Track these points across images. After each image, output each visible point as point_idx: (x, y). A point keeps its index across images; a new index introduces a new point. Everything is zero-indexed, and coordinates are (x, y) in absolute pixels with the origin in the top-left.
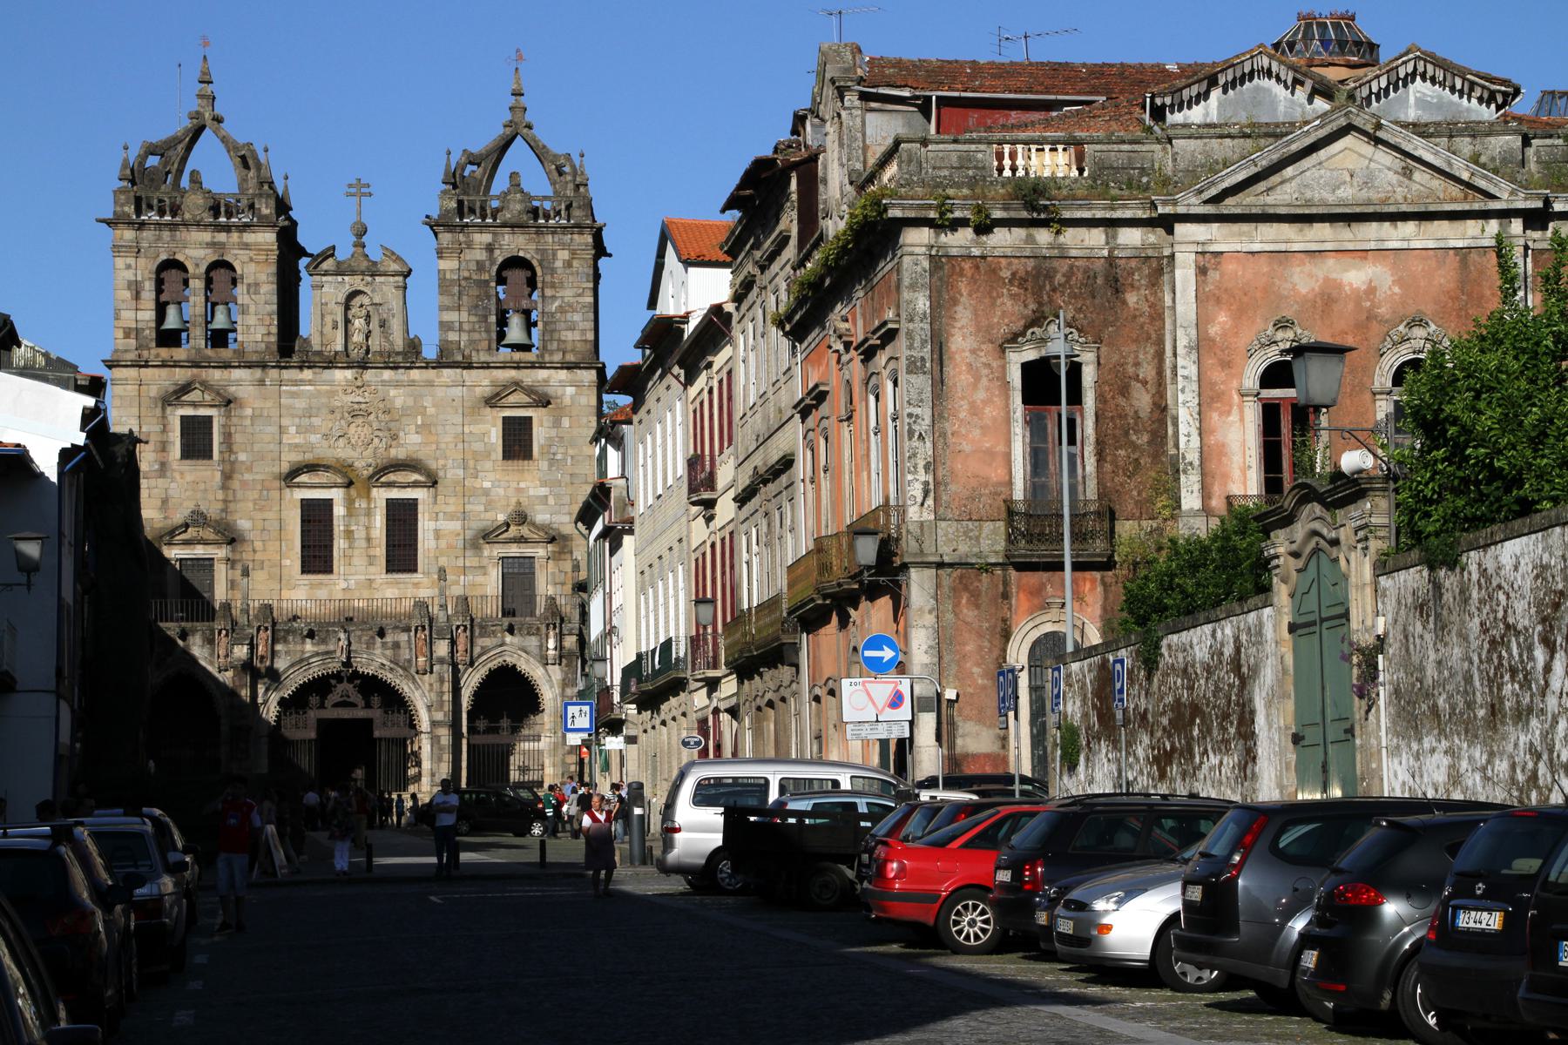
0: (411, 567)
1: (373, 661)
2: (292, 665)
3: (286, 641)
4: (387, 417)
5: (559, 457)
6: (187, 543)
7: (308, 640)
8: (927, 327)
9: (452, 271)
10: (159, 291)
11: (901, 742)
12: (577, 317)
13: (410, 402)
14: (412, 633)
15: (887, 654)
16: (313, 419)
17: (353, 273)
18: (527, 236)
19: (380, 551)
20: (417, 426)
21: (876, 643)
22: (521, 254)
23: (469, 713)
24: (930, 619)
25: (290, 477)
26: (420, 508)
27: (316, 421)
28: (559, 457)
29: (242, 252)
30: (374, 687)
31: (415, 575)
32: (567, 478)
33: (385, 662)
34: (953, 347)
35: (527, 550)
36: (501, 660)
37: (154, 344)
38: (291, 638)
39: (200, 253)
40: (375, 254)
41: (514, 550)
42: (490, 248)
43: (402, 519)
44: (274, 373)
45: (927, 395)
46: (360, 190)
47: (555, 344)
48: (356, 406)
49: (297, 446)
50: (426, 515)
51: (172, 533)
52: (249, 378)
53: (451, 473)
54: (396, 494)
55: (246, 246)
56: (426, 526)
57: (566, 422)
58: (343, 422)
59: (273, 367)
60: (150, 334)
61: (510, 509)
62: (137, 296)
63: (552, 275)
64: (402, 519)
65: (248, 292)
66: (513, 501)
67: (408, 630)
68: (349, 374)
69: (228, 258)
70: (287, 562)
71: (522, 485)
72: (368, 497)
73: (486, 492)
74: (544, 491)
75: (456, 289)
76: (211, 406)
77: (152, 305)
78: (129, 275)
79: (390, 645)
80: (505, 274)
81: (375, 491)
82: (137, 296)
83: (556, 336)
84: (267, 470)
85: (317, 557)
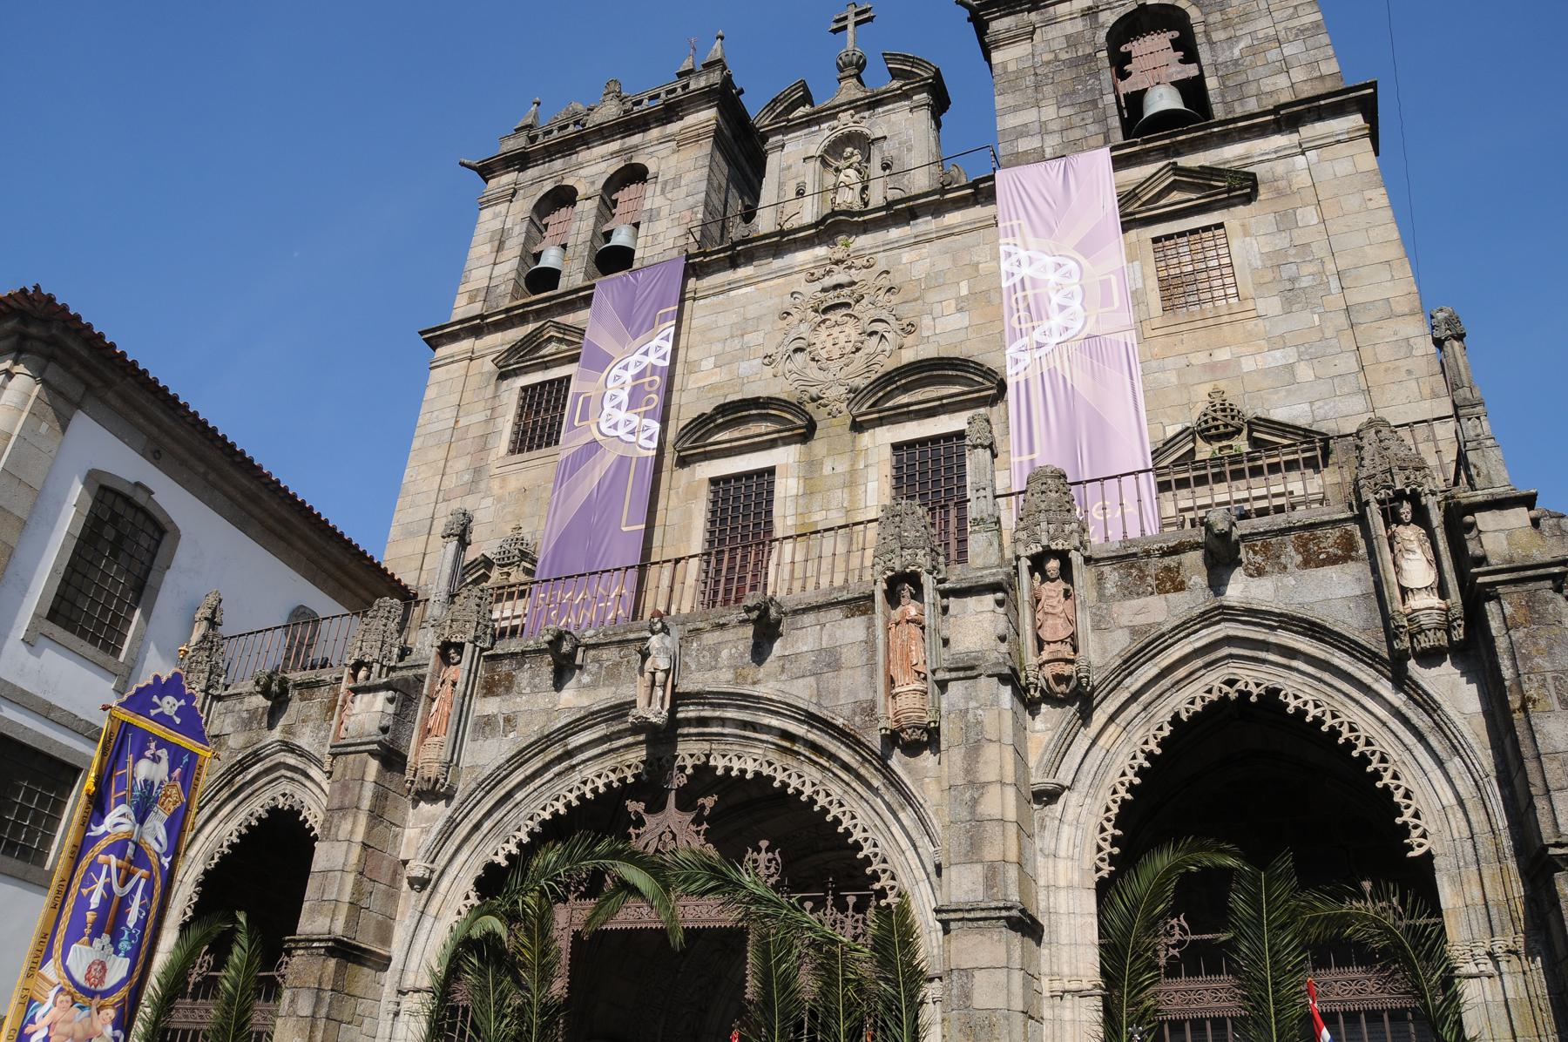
2: (519, 758)
4: (895, 299)
5: (1305, 282)
12: (1288, 50)
13: (944, 263)
16: (746, 338)
17: (832, 114)
20: (959, 299)
27: (753, 338)
28: (1305, 282)
29: (661, 146)
32: (1342, 320)
36: (1215, 678)
48: (832, 294)
49: (713, 387)
57: (1309, 216)
58: (804, 327)
61: (1202, 406)
62: (500, 248)
63: (1222, 11)
65: (663, 192)
67: (860, 605)
68: (821, 251)
69: (638, 159)
71: (1222, 355)
72: (854, 451)
74: (1278, 358)
75: (1029, 81)
77: (517, 251)
78: (497, 225)
79: (806, 663)
80: (1122, 49)
81: (866, 438)
82: (500, 248)
83: (1252, 89)
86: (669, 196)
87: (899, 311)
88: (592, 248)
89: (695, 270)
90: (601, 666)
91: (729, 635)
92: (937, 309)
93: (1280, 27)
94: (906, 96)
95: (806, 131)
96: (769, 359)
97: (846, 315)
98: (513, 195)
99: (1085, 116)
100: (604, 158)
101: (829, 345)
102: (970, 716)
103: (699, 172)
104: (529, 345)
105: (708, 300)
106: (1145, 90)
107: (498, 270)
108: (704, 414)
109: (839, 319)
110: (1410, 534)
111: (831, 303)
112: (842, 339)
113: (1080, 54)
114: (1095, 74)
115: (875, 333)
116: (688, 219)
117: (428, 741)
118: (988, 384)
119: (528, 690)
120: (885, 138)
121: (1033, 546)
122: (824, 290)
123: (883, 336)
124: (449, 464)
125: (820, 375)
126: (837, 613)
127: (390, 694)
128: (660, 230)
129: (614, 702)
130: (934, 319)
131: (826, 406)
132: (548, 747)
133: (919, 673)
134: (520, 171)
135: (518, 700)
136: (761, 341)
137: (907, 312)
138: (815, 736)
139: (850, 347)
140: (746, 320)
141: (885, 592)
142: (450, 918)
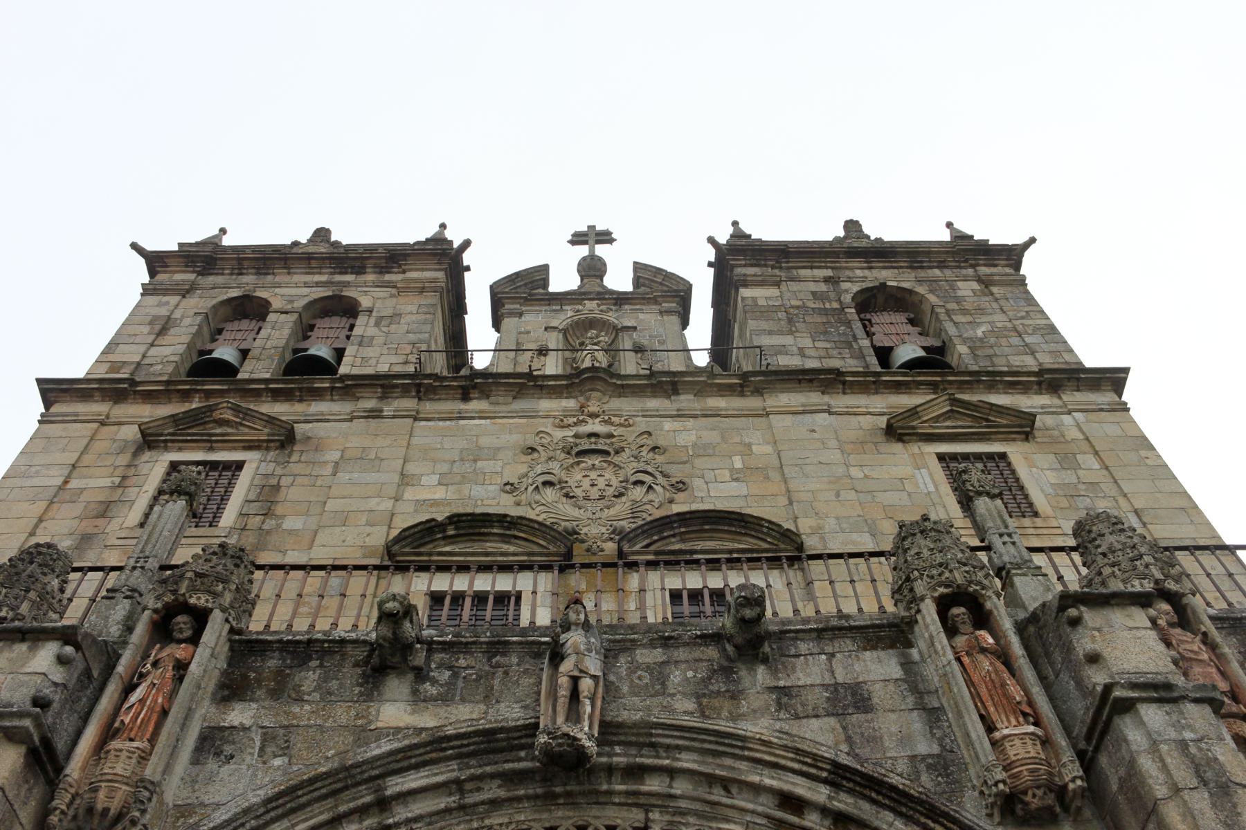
3: (280, 689)
4: (660, 459)
7: (397, 687)
16: (479, 464)
18: (896, 271)
20: (732, 470)
22: (889, 283)
33: (801, 787)
39: (306, 291)
48: (586, 440)
49: (435, 503)
52: (348, 411)
59: (405, 391)
65: (377, 324)
68: (571, 404)
75: (782, 315)
76: (250, 446)
77: (186, 339)
79: (818, 698)
82: (162, 332)
86: (385, 329)
87: (666, 468)
88: (282, 357)
89: (418, 392)
90: (455, 675)
91: (681, 654)
92: (710, 475)
93: (1017, 322)
94: (655, 301)
95: (547, 308)
96: (510, 487)
97: (604, 461)
98: (188, 291)
99: (841, 351)
100: (306, 285)
101: (586, 483)
102: (1193, 750)
103: (423, 317)
104: (194, 418)
105: (430, 423)
106: (890, 349)
107: (153, 351)
108: (433, 520)
109: (596, 462)
111: (587, 447)
112: (601, 483)
113: (827, 306)
114: (848, 324)
115: (642, 483)
116: (409, 352)
117: (115, 744)
118: (783, 546)
119: (317, 696)
120: (635, 328)
121: (1136, 582)
122: (576, 436)
123: (650, 487)
124: (43, 525)
125: (576, 513)
126: (848, 644)
127: (69, 649)
128: (371, 354)
129: (483, 725)
130: (707, 483)
131: (583, 541)
132: (346, 788)
133: (1025, 715)
134: (199, 274)
135: (298, 710)
136: (500, 470)
137: (677, 472)
138: (845, 803)
139: (611, 491)
140: (480, 448)
141: (939, 613)
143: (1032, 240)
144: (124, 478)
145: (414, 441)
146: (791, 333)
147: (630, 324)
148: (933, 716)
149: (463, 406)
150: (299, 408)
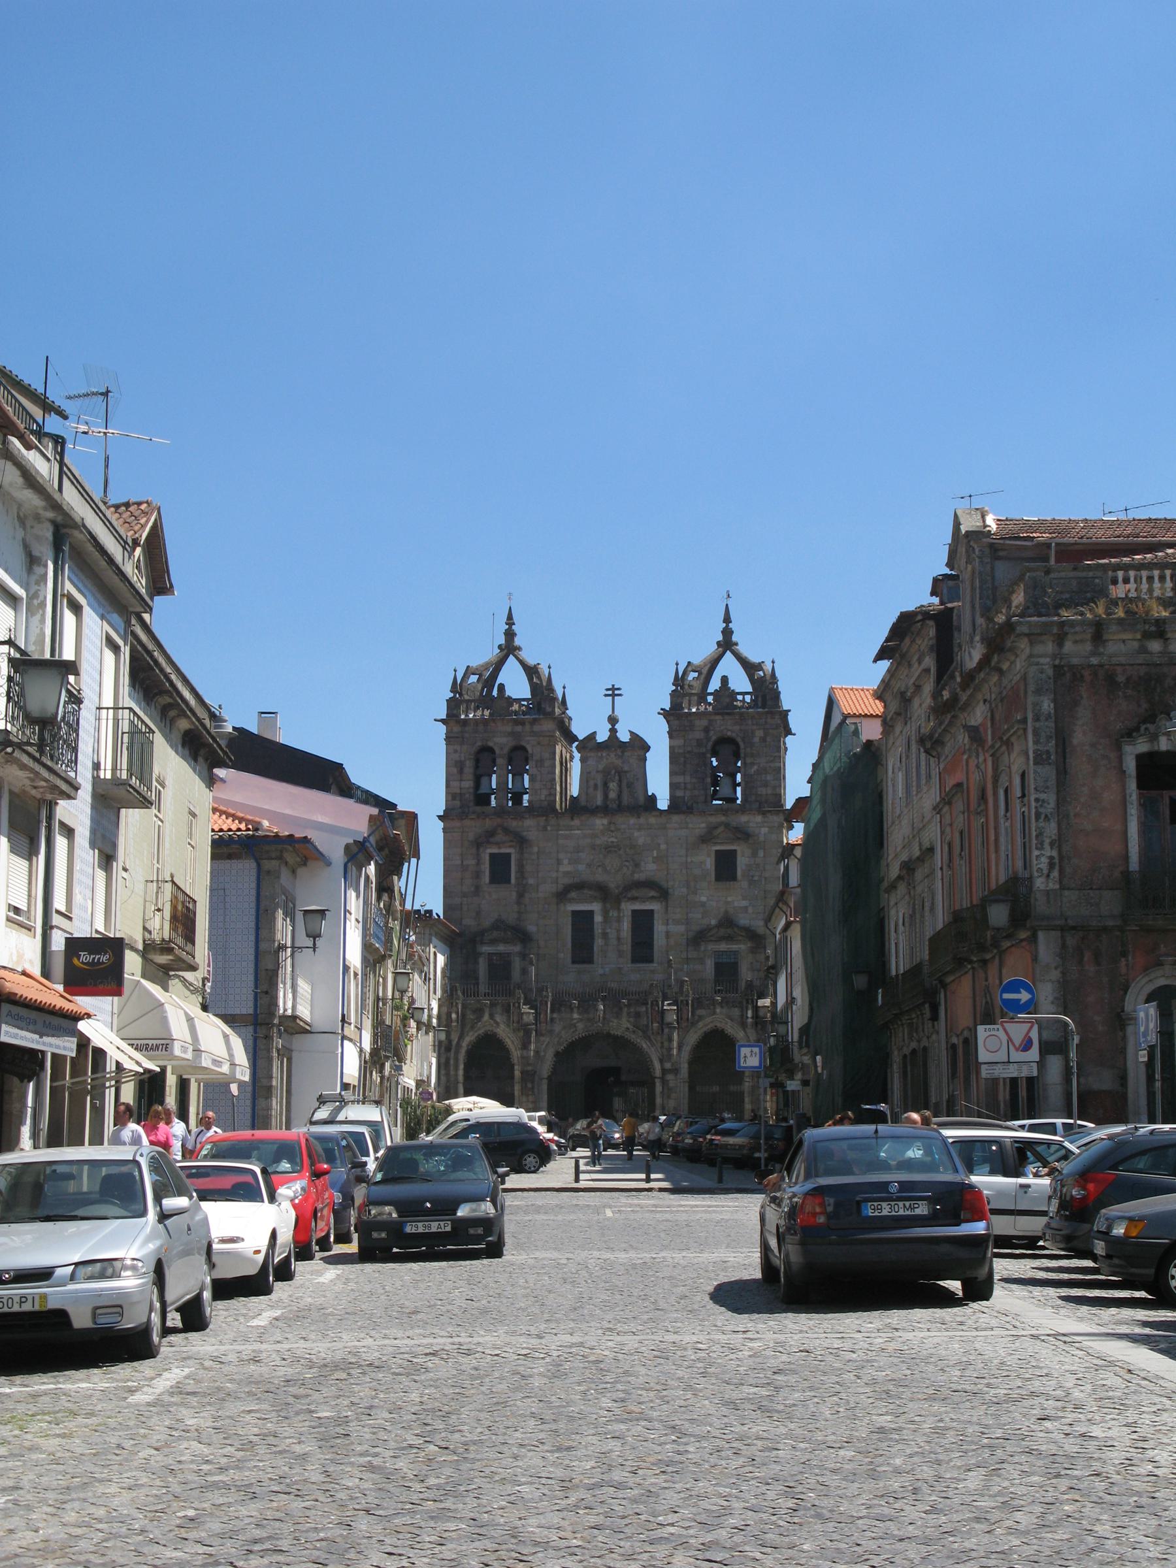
0: (649, 959)
1: (622, 1026)
3: (559, 1011)
6: (493, 942)
8: (1053, 725)
9: (679, 747)
10: (477, 767)
11: (1030, 1081)
12: (769, 777)
14: (649, 1006)
15: (1024, 996)
16: (581, 854)
19: (627, 947)
20: (653, 857)
21: (1014, 987)
22: (729, 733)
23: (690, 1063)
24: (1055, 975)
25: (562, 895)
26: (656, 916)
28: (756, 878)
30: (620, 1043)
31: (651, 965)
33: (629, 1026)
34: (1075, 741)
35: (734, 947)
37: (472, 804)
38: (563, 1009)
40: (624, 737)
41: (723, 946)
42: (706, 730)
43: (643, 923)
44: (553, 821)
45: (1052, 782)
46: (613, 692)
47: (753, 798)
49: (568, 873)
50: (660, 922)
51: (482, 933)
53: (678, 890)
54: (638, 906)
55: (533, 734)
56: (659, 928)
57: (761, 853)
60: (469, 797)
64: (643, 923)
66: (722, 910)
68: (605, 821)
69: (523, 744)
70: (561, 955)
71: (729, 899)
72: (619, 909)
73: (703, 904)
74: (744, 903)
76: (510, 847)
77: (471, 777)
78: (456, 757)
84: (547, 889)
85: (583, 950)
110: (750, 1006)
142: (549, 1063)
143: (789, 711)
144: (479, 860)
145: (561, 842)
146: (683, 774)
147: (626, 768)
148: (648, 1017)
149: (572, 823)
150: (520, 823)
